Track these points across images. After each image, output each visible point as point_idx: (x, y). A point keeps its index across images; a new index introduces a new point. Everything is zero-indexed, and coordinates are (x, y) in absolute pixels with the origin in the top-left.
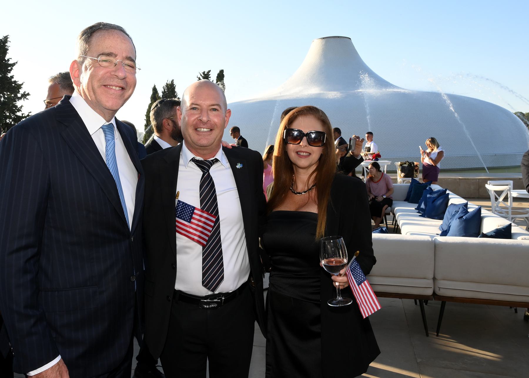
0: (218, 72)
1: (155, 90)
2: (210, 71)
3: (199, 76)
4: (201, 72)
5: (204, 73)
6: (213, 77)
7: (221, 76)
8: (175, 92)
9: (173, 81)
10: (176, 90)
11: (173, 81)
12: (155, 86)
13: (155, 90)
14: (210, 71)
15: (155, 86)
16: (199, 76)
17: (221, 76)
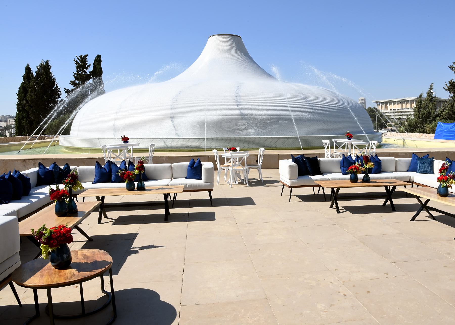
0: (96, 56)
1: (28, 69)
2: (87, 55)
3: (76, 59)
4: (78, 55)
5: (81, 56)
6: (90, 61)
7: (98, 60)
8: (50, 73)
9: (47, 62)
10: (51, 70)
11: (47, 62)
12: (28, 65)
13: (28, 69)
14: (87, 55)
15: (28, 65)
16: (76, 59)
17: (98, 60)
